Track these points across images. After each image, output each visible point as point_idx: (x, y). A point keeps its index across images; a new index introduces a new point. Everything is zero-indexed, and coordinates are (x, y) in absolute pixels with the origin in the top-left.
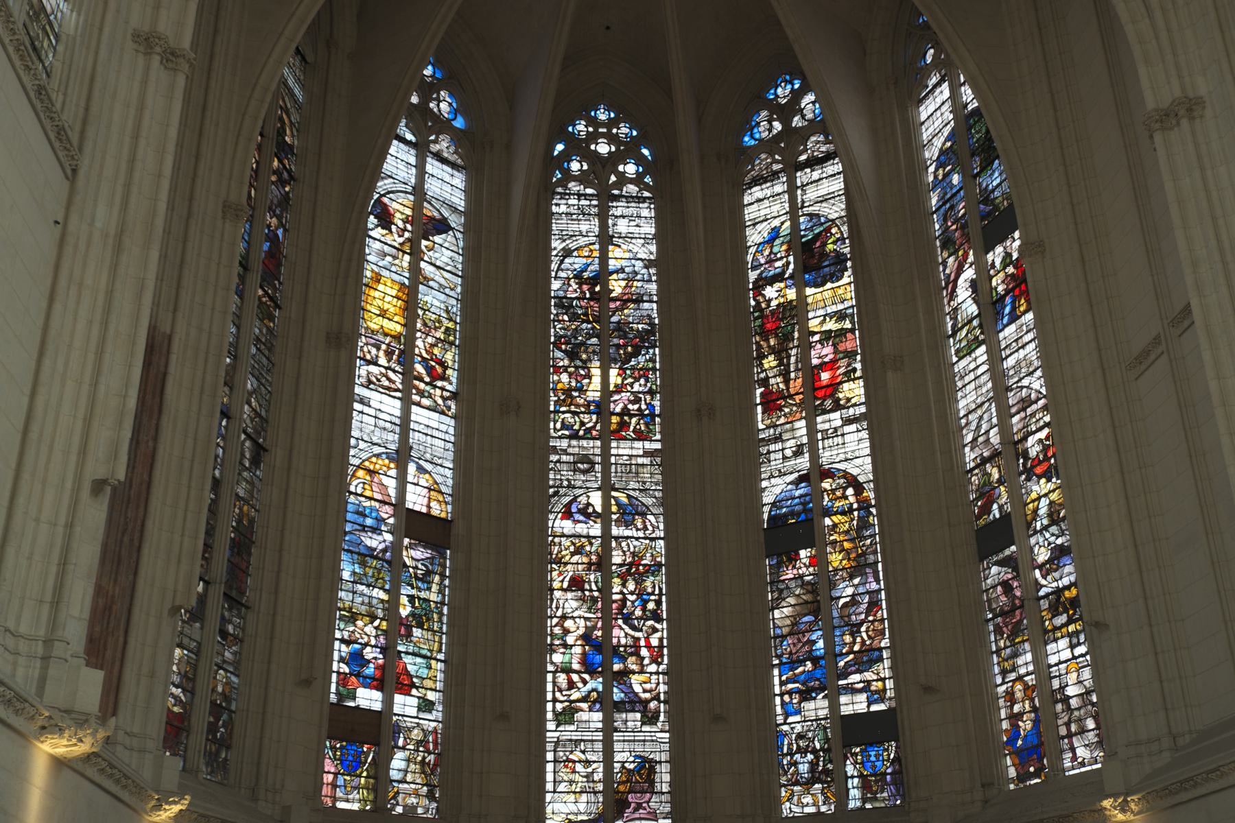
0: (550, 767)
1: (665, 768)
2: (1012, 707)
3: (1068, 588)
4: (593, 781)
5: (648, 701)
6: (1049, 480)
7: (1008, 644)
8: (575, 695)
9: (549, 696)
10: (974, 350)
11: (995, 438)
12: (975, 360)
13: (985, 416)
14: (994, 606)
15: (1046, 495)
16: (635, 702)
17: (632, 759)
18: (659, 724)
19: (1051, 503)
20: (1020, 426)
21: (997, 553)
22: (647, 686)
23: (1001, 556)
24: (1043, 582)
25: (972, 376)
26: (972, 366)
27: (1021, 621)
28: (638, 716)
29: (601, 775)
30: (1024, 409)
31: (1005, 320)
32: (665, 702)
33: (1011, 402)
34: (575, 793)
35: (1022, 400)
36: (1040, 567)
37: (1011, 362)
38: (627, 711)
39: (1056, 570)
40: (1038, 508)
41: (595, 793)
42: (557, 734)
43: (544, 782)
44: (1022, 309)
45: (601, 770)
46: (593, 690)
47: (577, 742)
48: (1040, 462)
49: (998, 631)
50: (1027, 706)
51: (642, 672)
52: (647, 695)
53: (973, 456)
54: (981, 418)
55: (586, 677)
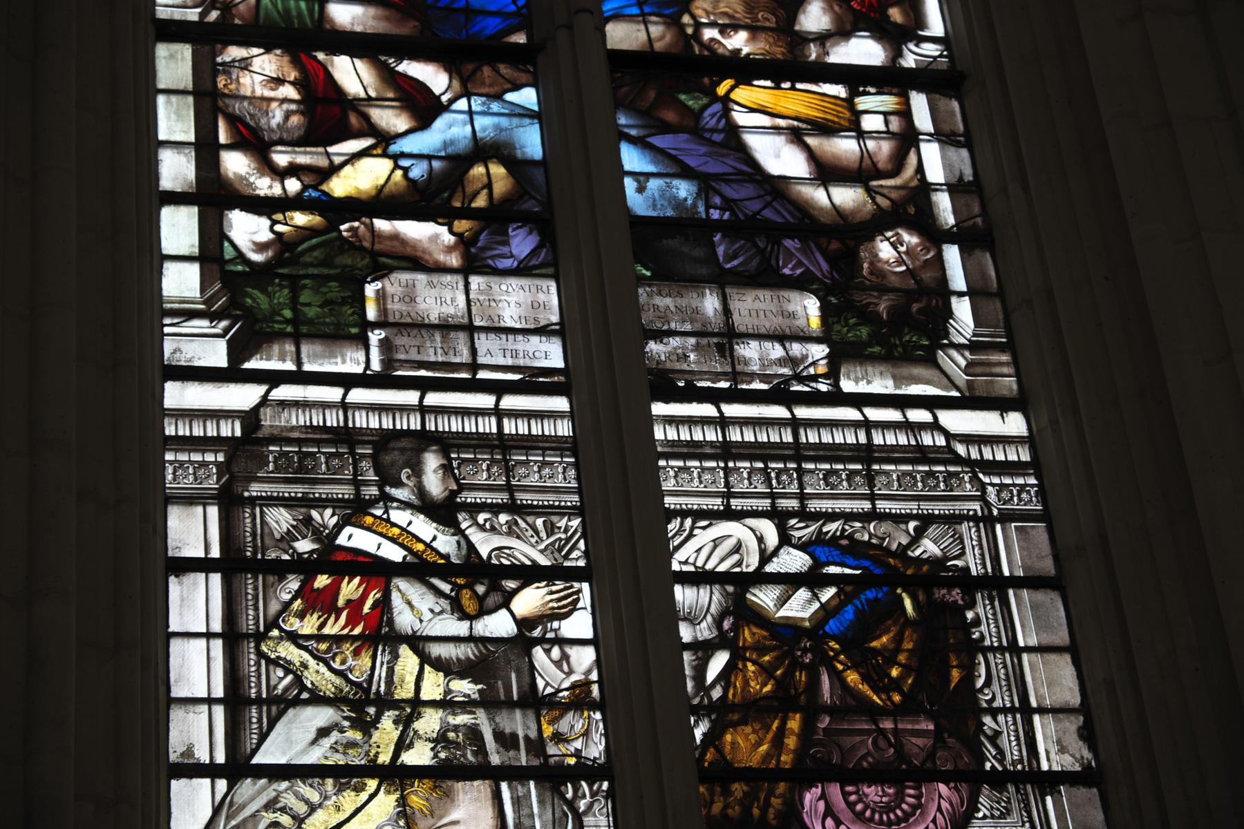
0: (194, 604)
1: (1031, 620)
4: (533, 701)
5: (851, 233)
8: (362, 176)
9: (176, 170)
16: (776, 233)
17: (793, 561)
18: (955, 363)
22: (845, 147)
28: (809, 308)
29: (584, 658)
32: (964, 237)
34: (396, 775)
38: (723, 281)
41: (553, 777)
42: (244, 396)
43: (159, 701)
45: (580, 625)
46: (482, 151)
47: (394, 451)
51: (792, 64)
52: (846, 196)
55: (434, 77)
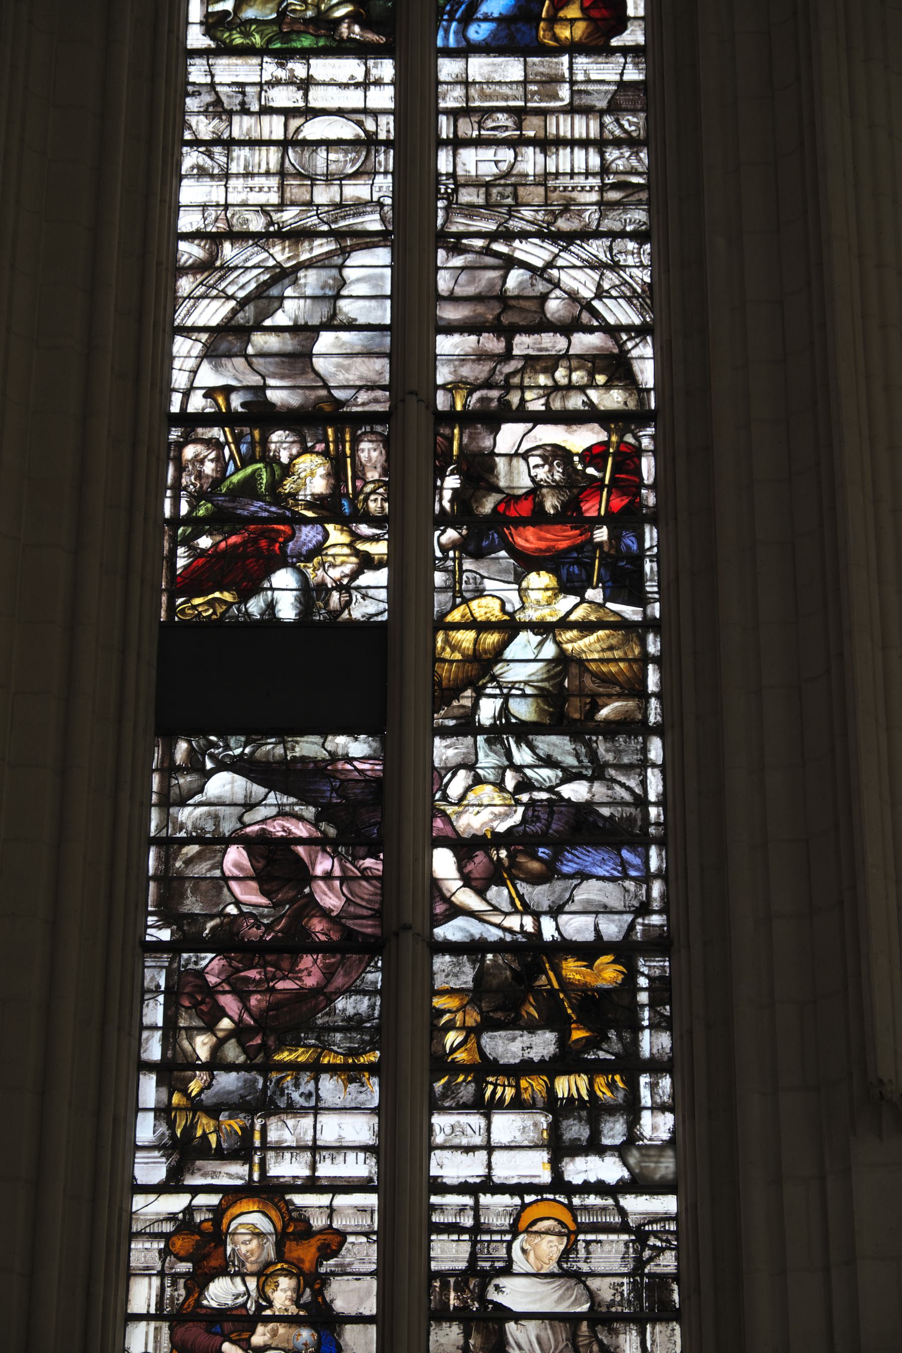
2: (198, 1283)
3: (588, 952)
6: (565, 587)
7: (232, 1052)
10: (306, 54)
11: (345, 364)
12: (306, 84)
13: (311, 280)
14: (193, 905)
15: (542, 628)
19: (563, 661)
20: (471, 372)
21: (255, 733)
23: (272, 749)
24: (467, 898)
25: (274, 128)
26: (284, 97)
27: (323, 996)
30: (507, 332)
31: (478, 32)
33: (444, 282)
35: (502, 298)
36: (465, 847)
37: (475, 162)
39: (536, 880)
40: (497, 655)
44: (564, 33)
48: (539, 518)
49: (192, 999)
50: (282, 1294)
53: (208, 377)
54: (284, 274)
